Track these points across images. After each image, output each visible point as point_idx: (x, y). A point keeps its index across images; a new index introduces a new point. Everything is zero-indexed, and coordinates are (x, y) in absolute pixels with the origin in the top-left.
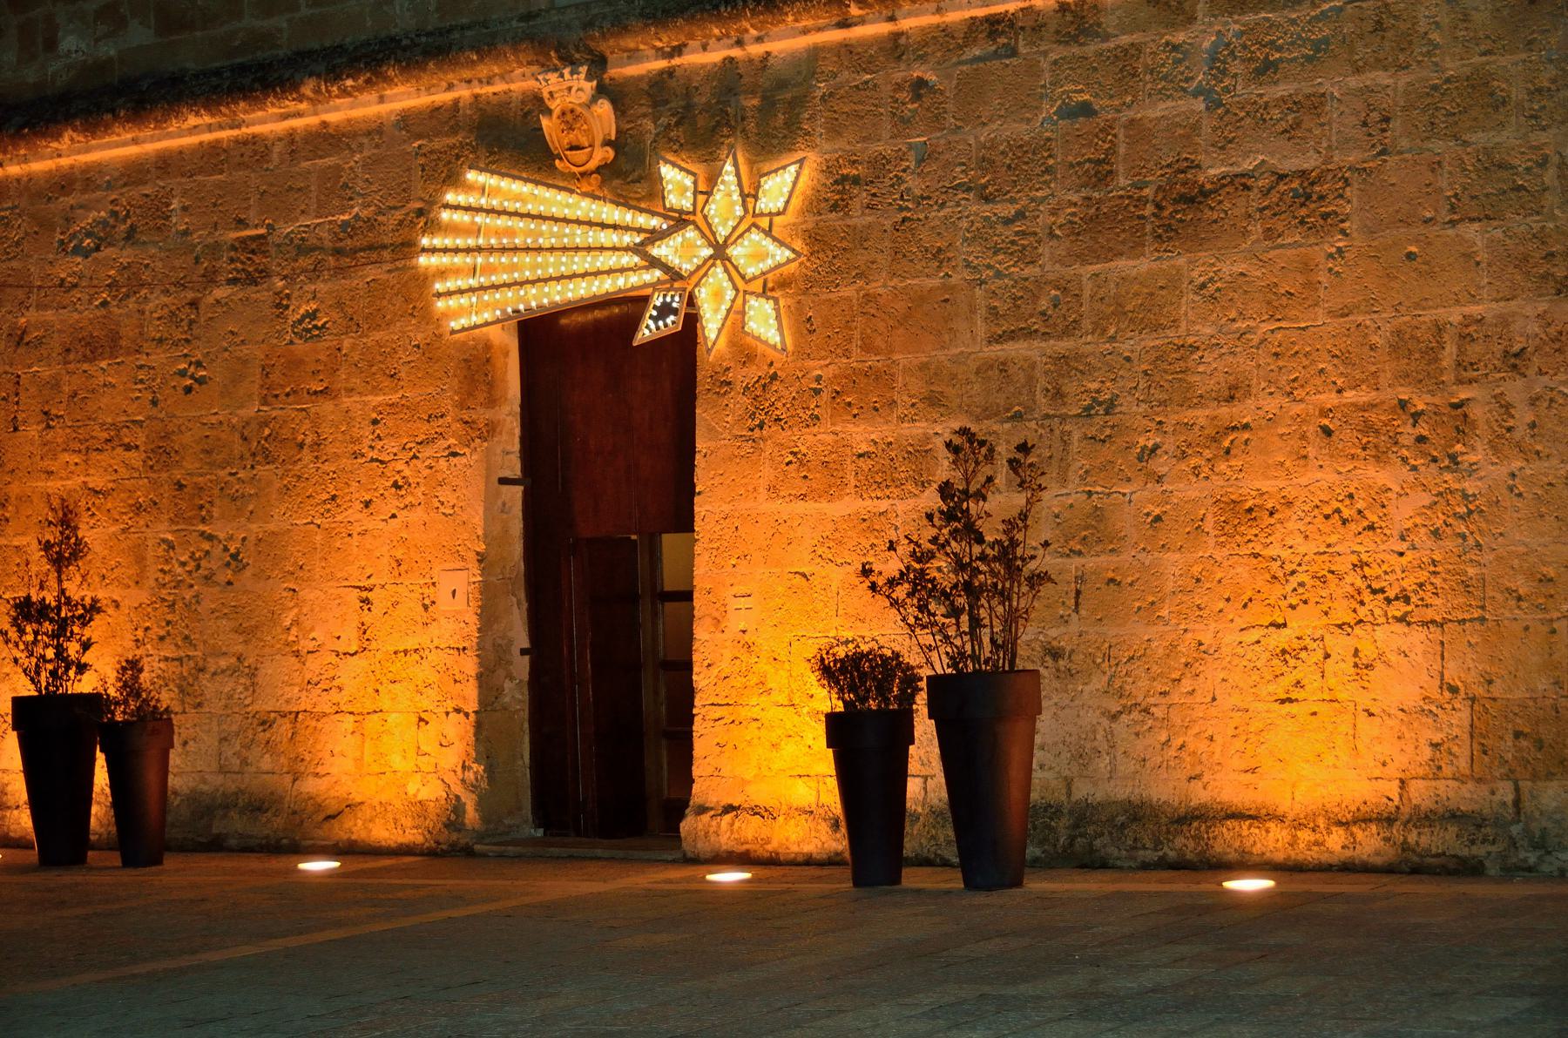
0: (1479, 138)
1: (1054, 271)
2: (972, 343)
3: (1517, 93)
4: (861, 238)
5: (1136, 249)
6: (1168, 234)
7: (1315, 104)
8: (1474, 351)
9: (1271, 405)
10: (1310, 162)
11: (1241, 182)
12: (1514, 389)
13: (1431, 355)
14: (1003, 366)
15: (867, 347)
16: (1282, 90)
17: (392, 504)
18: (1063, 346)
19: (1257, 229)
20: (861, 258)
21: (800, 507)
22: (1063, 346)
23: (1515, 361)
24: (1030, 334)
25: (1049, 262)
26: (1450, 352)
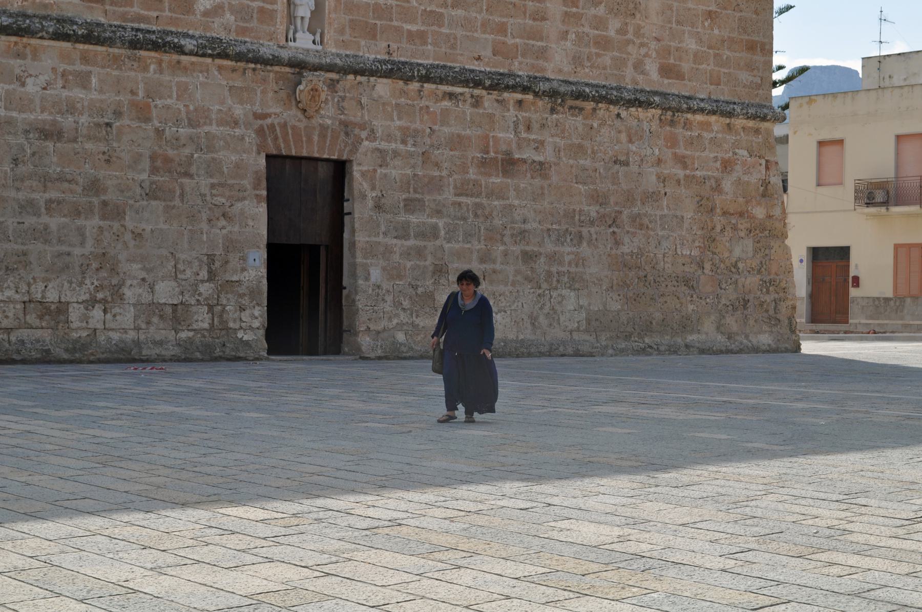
0: (582, 162)
1: (473, 177)
2: (448, 195)
3: (589, 152)
4: (411, 155)
5: (497, 176)
6: (506, 173)
7: (542, 143)
8: (582, 218)
9: (535, 225)
10: (542, 159)
11: (524, 161)
12: (593, 230)
13: (573, 218)
14: (459, 204)
15: (415, 191)
16: (533, 137)
17: (223, 222)
18: (478, 200)
19: (529, 175)
20: (412, 161)
21: (395, 241)
22: (478, 200)
23: (592, 223)
24: (467, 195)
25: (472, 174)
26: (577, 217)
